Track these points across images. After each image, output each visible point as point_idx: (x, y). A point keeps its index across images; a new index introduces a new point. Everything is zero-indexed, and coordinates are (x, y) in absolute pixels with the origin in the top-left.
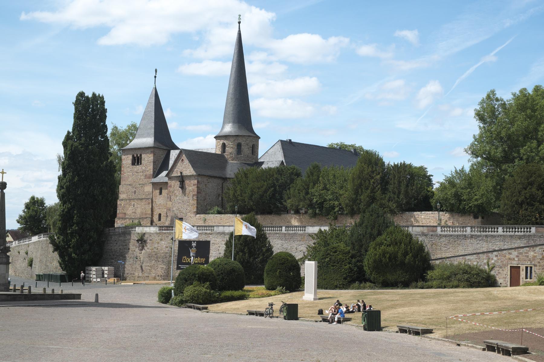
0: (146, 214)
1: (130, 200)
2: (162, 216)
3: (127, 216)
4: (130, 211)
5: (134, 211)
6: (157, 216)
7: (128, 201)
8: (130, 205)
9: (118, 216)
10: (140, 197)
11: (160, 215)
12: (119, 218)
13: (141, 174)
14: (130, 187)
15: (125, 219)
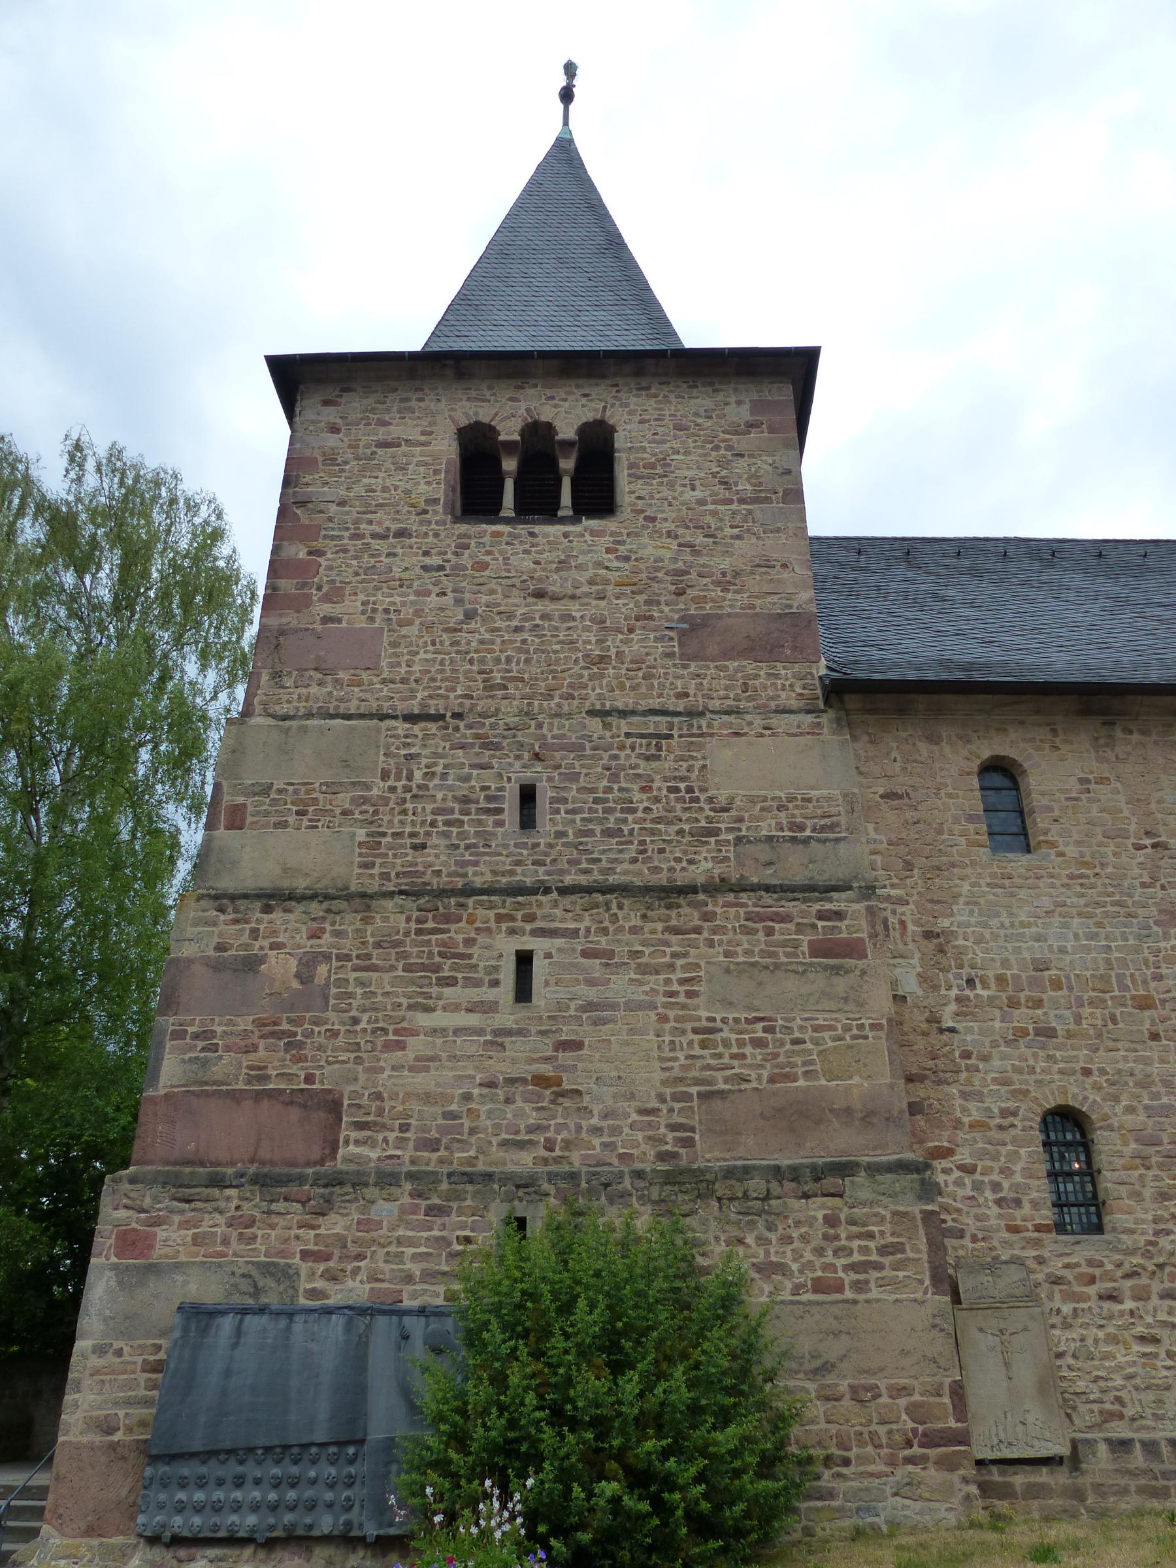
0: (798, 1115)
1: (437, 899)
2: (1111, 1147)
3: (356, 1151)
4: (433, 1061)
5: (520, 1058)
6: (1024, 1163)
7: (394, 917)
8: (438, 971)
9: (159, 1139)
10: (639, 875)
11: (1067, 1127)
12: (195, 1181)
13: (627, 606)
14: (428, 742)
15: (338, 1185)
